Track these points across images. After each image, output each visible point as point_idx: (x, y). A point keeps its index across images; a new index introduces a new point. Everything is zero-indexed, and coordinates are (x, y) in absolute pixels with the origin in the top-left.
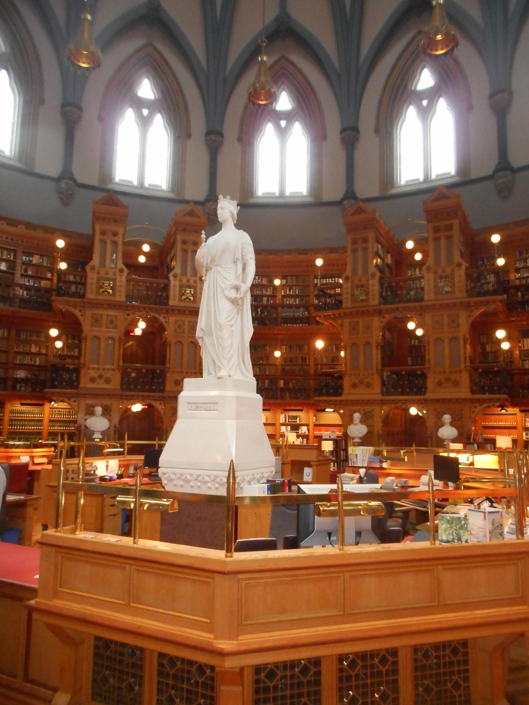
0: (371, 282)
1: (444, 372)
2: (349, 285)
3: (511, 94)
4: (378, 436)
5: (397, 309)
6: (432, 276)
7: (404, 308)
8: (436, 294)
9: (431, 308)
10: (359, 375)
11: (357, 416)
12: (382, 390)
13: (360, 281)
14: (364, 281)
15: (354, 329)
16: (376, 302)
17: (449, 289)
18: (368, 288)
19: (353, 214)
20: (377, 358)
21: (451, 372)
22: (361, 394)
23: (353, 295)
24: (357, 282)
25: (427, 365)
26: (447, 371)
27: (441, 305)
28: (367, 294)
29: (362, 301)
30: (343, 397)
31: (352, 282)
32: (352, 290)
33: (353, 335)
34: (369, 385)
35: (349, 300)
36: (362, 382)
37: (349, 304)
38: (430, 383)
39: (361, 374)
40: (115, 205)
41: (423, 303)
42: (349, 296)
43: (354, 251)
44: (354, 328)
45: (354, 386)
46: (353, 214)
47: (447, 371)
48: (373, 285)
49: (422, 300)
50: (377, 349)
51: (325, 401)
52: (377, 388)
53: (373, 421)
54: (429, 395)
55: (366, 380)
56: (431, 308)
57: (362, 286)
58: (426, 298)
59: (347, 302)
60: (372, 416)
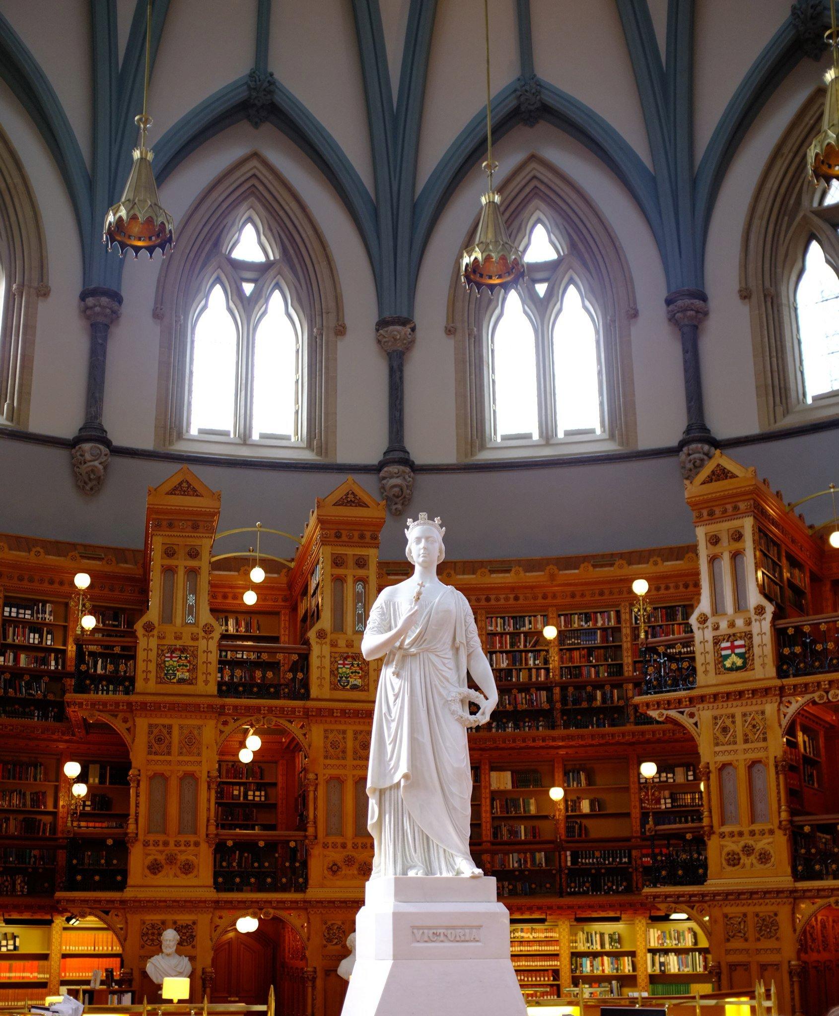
0: (202, 644)
1: (344, 846)
2: (153, 643)
3: (413, 329)
4: (204, 980)
5: (258, 709)
6: (327, 649)
7: (270, 709)
8: (334, 687)
9: (321, 714)
10: (166, 844)
11: (170, 936)
12: (215, 882)
13: (178, 637)
14: (187, 641)
15: (159, 741)
16: (213, 689)
17: (359, 682)
18: (195, 656)
19: (172, 492)
20: (209, 809)
21: (355, 846)
22: (169, 885)
23: (160, 666)
24: (170, 641)
25: (311, 831)
26: (349, 845)
27: (343, 712)
28: (193, 669)
29: (181, 681)
30: (129, 893)
31: (161, 637)
32: (158, 655)
33: (156, 754)
34: (187, 868)
35: (152, 676)
36: (171, 860)
37: (152, 686)
38: (316, 867)
39: (172, 843)
40: (196, 485)
41: (309, 704)
42: (152, 667)
43: (169, 571)
44: (159, 740)
45: (155, 868)
46: (172, 492)
47: (349, 845)
48: (207, 652)
49: (306, 696)
50: (209, 788)
51: (85, 901)
52: (205, 873)
53: (193, 947)
54: (314, 893)
55: (182, 858)
56: (321, 714)
57: (183, 650)
58: (314, 692)
59: (146, 680)
60: (193, 937)
